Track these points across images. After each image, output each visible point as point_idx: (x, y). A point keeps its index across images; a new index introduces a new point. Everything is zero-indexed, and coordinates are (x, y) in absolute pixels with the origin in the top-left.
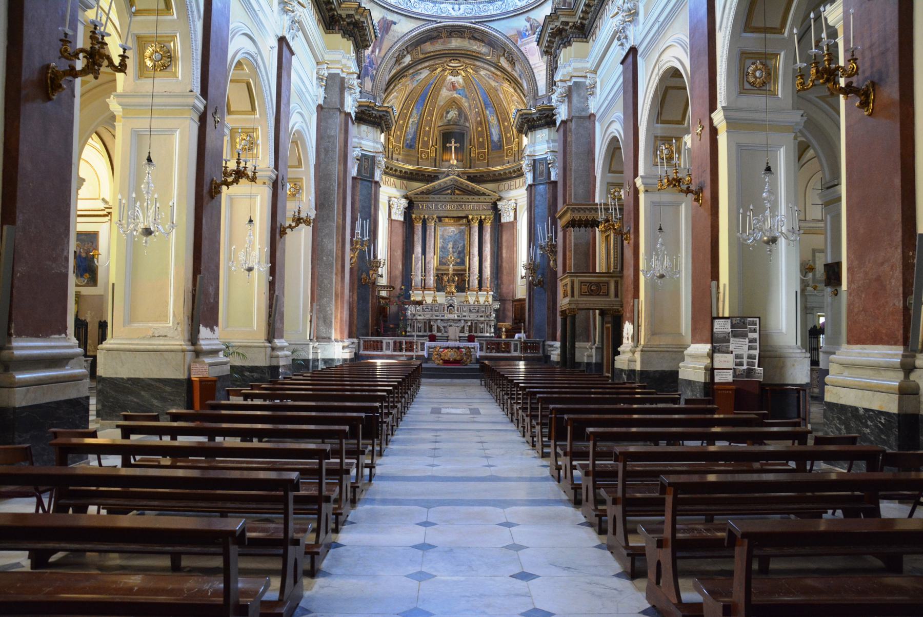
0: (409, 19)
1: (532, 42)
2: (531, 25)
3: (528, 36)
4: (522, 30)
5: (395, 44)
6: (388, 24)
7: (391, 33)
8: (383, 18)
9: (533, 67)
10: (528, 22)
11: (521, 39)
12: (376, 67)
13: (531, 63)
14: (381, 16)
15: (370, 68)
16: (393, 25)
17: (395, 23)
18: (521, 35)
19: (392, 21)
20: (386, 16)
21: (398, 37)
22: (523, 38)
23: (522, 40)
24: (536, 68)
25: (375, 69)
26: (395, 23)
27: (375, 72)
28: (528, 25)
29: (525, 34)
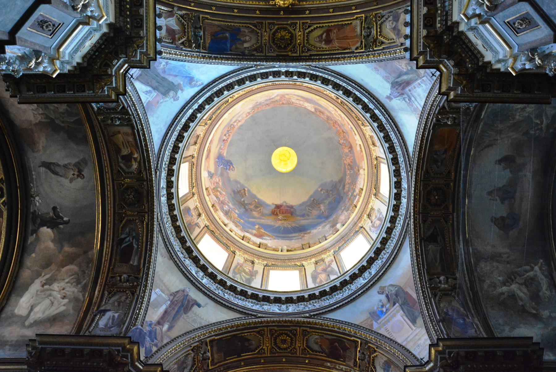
0: (219, 307)
1: (394, 315)
2: (387, 296)
3: (386, 313)
4: (375, 308)
5: (194, 330)
6: (188, 301)
7: (190, 314)
8: (183, 291)
9: (403, 344)
10: (382, 293)
11: (376, 322)
12: (160, 345)
13: (399, 341)
14: (181, 287)
15: (148, 339)
16: (195, 307)
17: (199, 306)
18: (375, 315)
19: (195, 301)
20: (188, 290)
21: (200, 323)
22: (380, 318)
23: (379, 322)
24: (409, 342)
25: (156, 345)
26: (199, 306)
27: (154, 349)
28: (383, 297)
29: (382, 312)
